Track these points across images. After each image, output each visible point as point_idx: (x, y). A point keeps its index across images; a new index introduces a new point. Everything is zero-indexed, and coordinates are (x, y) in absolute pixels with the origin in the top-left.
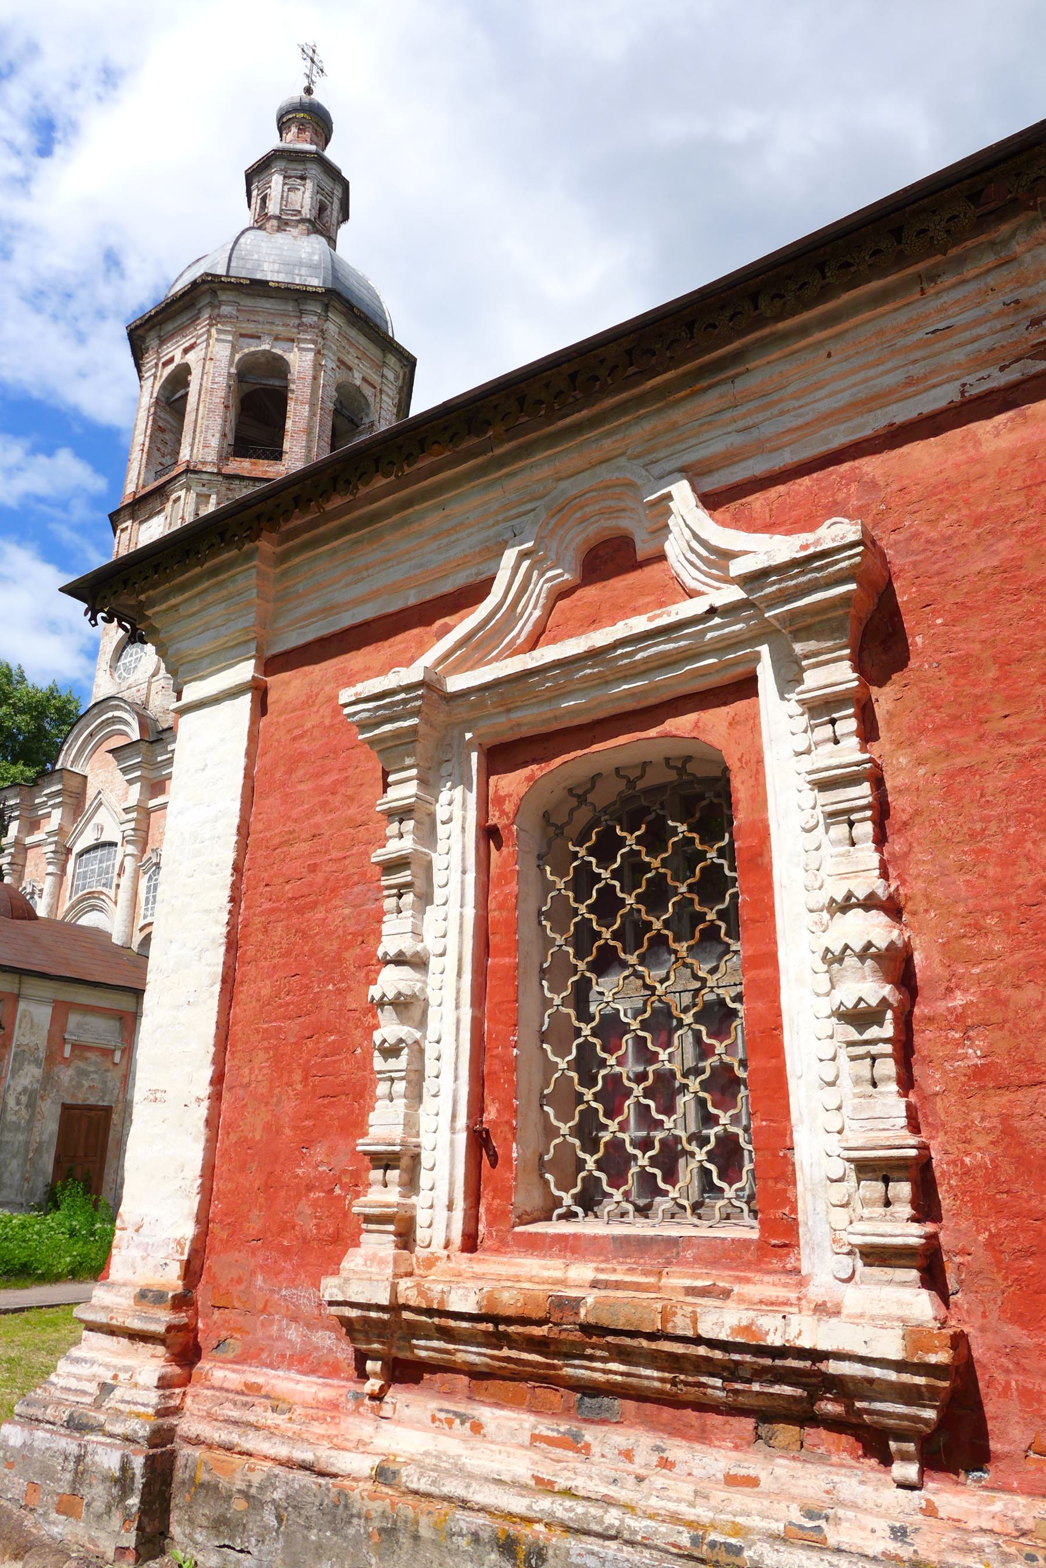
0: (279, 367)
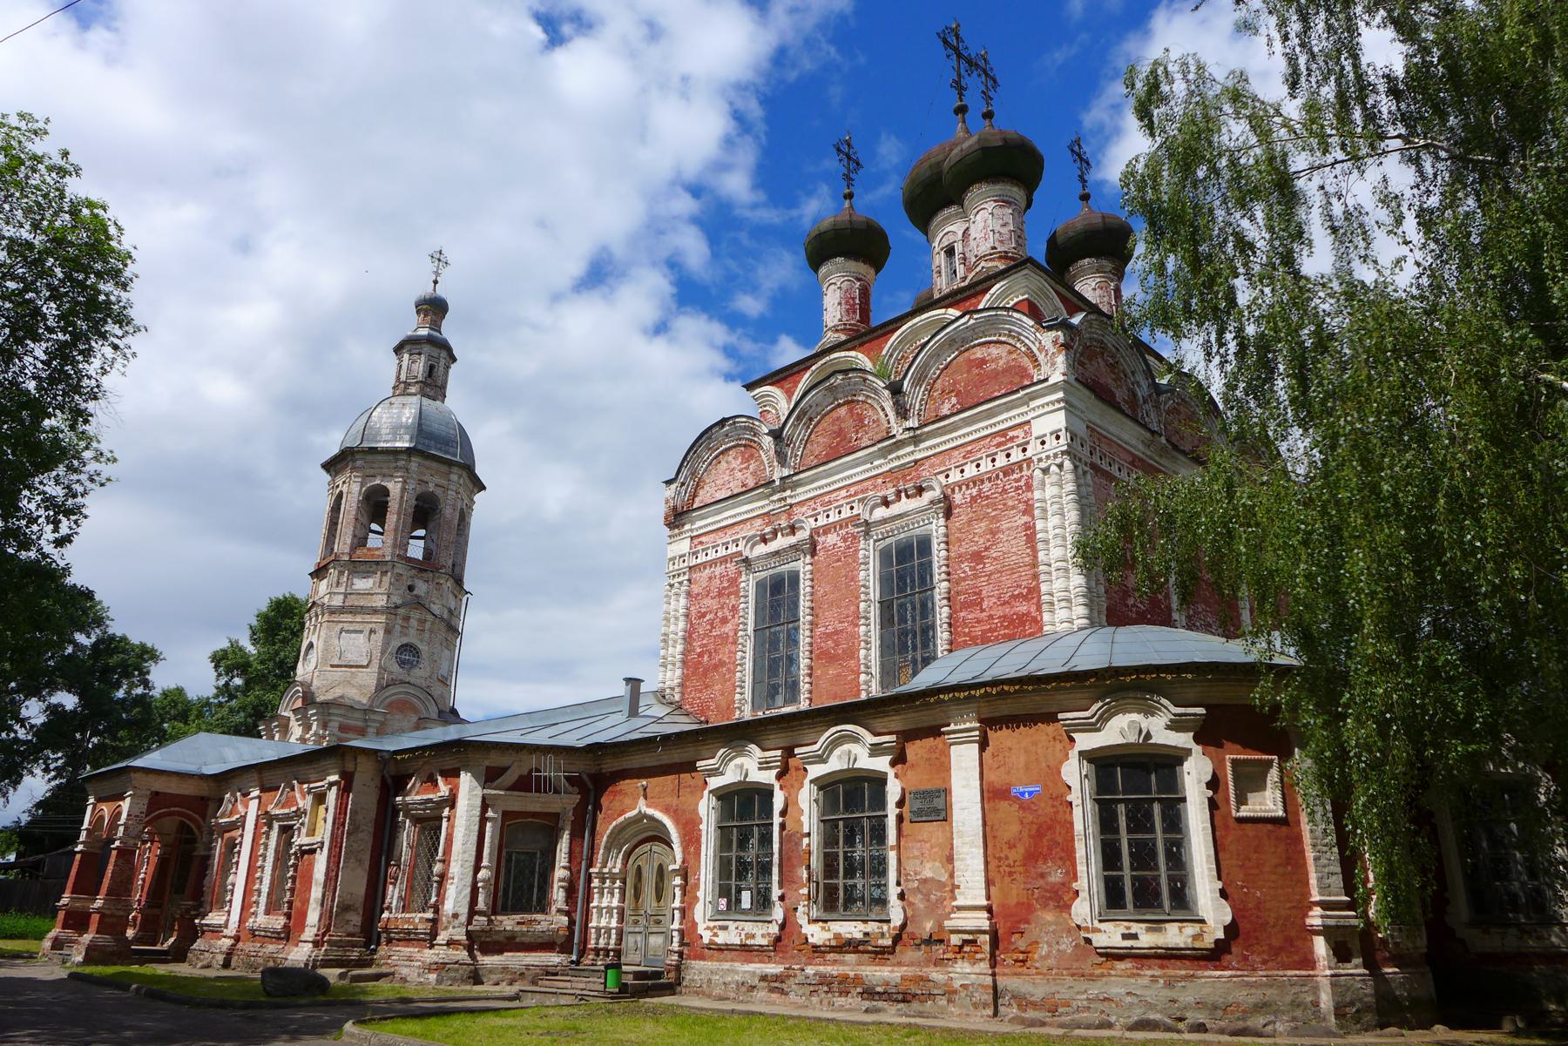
0: (385, 492)
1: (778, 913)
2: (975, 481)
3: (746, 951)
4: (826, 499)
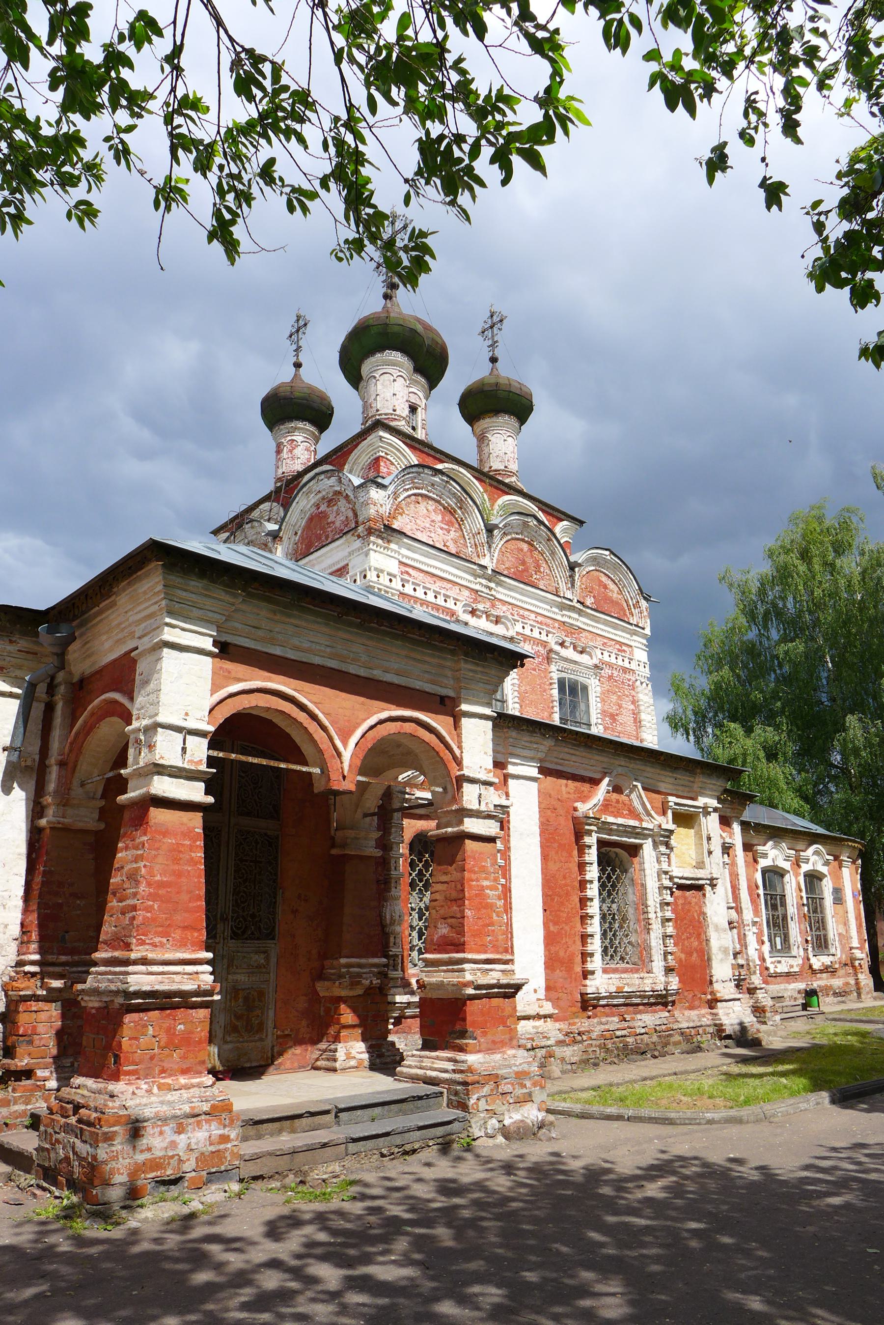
4: (522, 612)
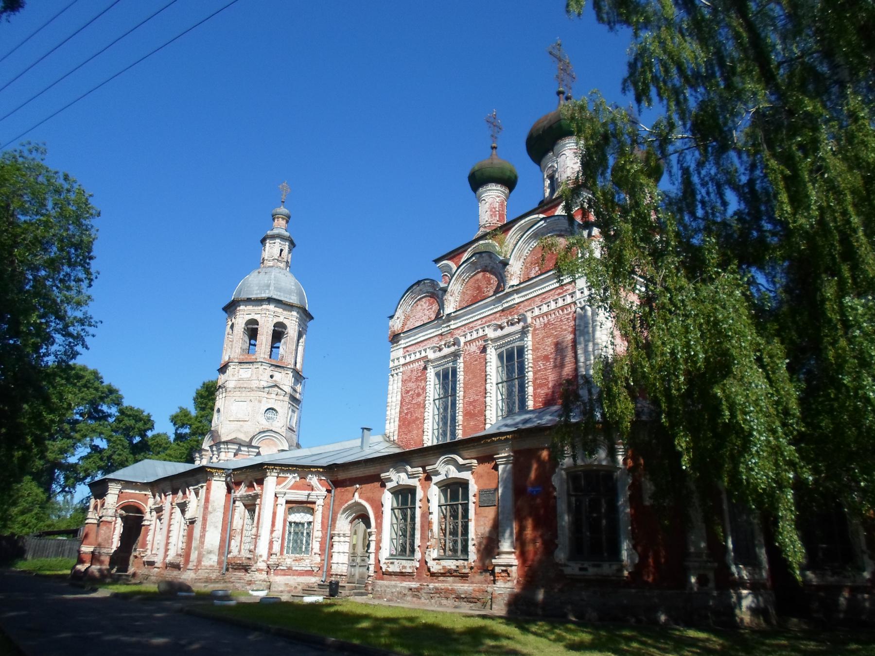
1: (418, 555)
2: (546, 314)
3: (402, 575)
4: (471, 325)
